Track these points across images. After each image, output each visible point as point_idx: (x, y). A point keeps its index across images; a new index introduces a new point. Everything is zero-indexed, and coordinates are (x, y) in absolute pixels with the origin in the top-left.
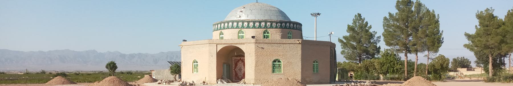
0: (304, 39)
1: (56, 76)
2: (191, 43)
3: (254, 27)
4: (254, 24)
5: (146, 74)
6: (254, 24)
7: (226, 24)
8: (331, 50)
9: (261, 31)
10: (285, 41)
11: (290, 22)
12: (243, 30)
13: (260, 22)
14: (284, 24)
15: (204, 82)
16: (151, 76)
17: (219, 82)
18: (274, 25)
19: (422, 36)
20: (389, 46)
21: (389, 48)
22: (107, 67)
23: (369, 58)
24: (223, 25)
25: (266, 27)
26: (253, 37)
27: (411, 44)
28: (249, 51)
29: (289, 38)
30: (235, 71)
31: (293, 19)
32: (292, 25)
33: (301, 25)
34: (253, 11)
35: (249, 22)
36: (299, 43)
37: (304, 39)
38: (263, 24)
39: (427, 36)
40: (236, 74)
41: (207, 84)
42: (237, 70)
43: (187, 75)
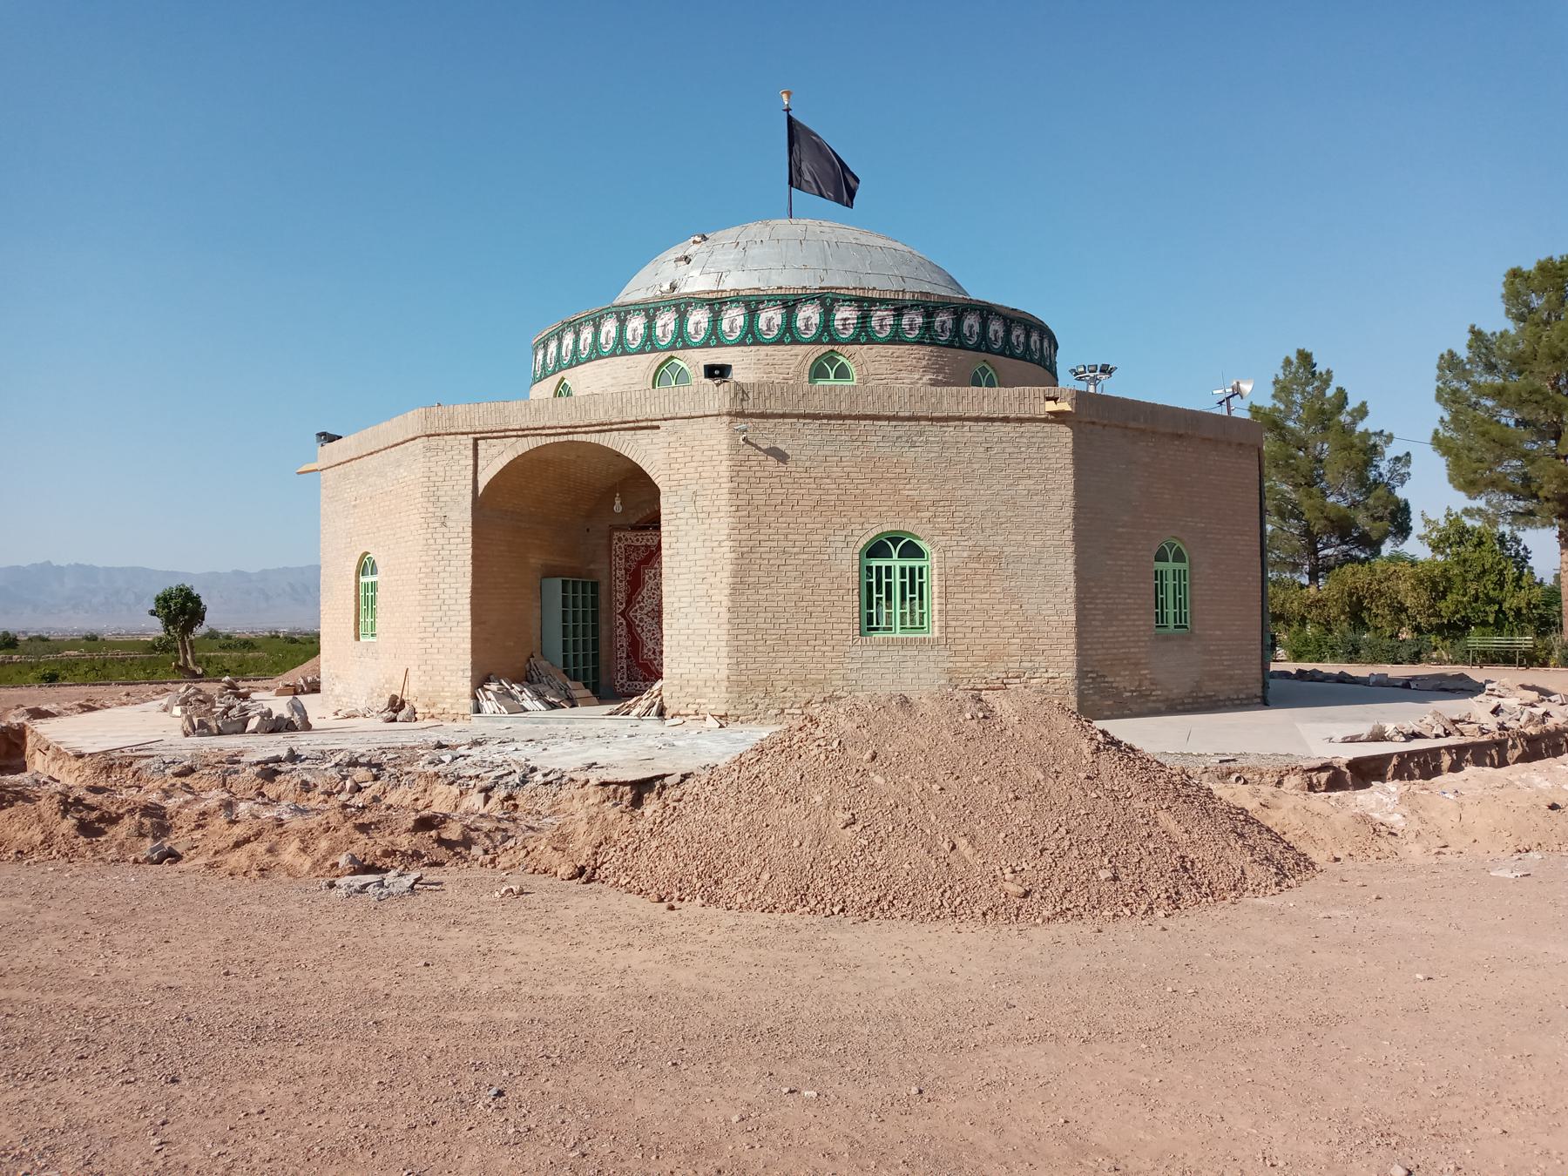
13: (790, 304)
14: (943, 319)
18: (881, 319)
38: (809, 315)
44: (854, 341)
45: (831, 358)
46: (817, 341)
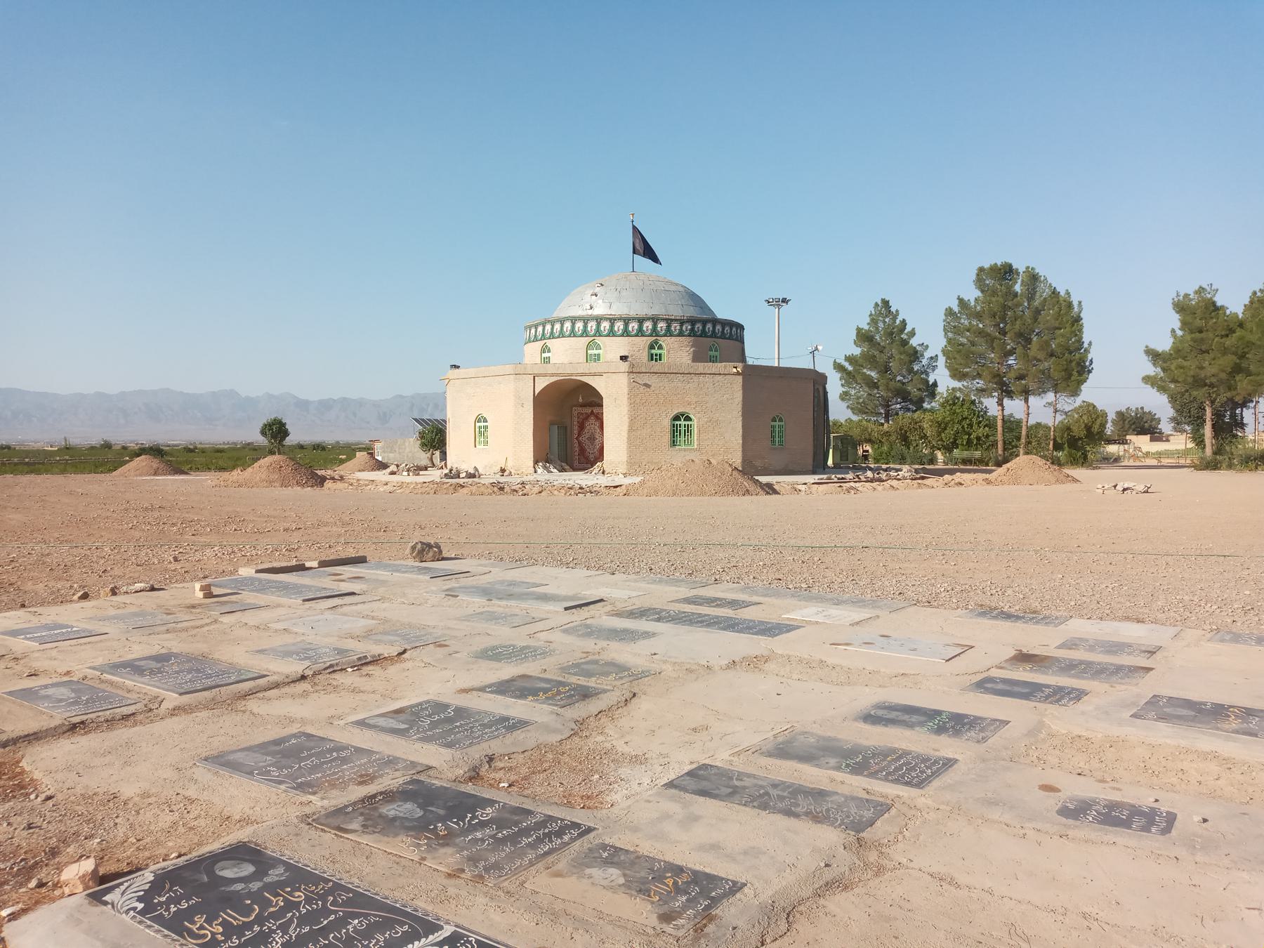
0: (750, 362)
1: (139, 455)
2: (472, 372)
3: (626, 333)
4: (626, 325)
5: (361, 450)
6: (626, 325)
7: (557, 326)
8: (816, 391)
9: (644, 342)
10: (701, 367)
11: (715, 321)
12: (599, 340)
13: (641, 321)
14: (699, 326)
15: (503, 471)
16: (372, 455)
17: (540, 471)
18: (675, 327)
19: (1041, 355)
20: (959, 380)
21: (957, 384)
22: (263, 433)
23: (908, 410)
24: (548, 327)
25: (654, 332)
26: (624, 358)
27: (1012, 375)
28: (614, 392)
29: (713, 360)
30: (580, 443)
31: (720, 315)
32: (718, 327)
33: (741, 327)
34: (624, 293)
35: (612, 321)
36: (738, 373)
37: (750, 362)
38: (648, 325)
39: (1052, 355)
40: (582, 451)
41: (510, 474)
42: (584, 438)
43: (460, 452)
44: (665, 335)
45: (656, 342)
46: (651, 335)
